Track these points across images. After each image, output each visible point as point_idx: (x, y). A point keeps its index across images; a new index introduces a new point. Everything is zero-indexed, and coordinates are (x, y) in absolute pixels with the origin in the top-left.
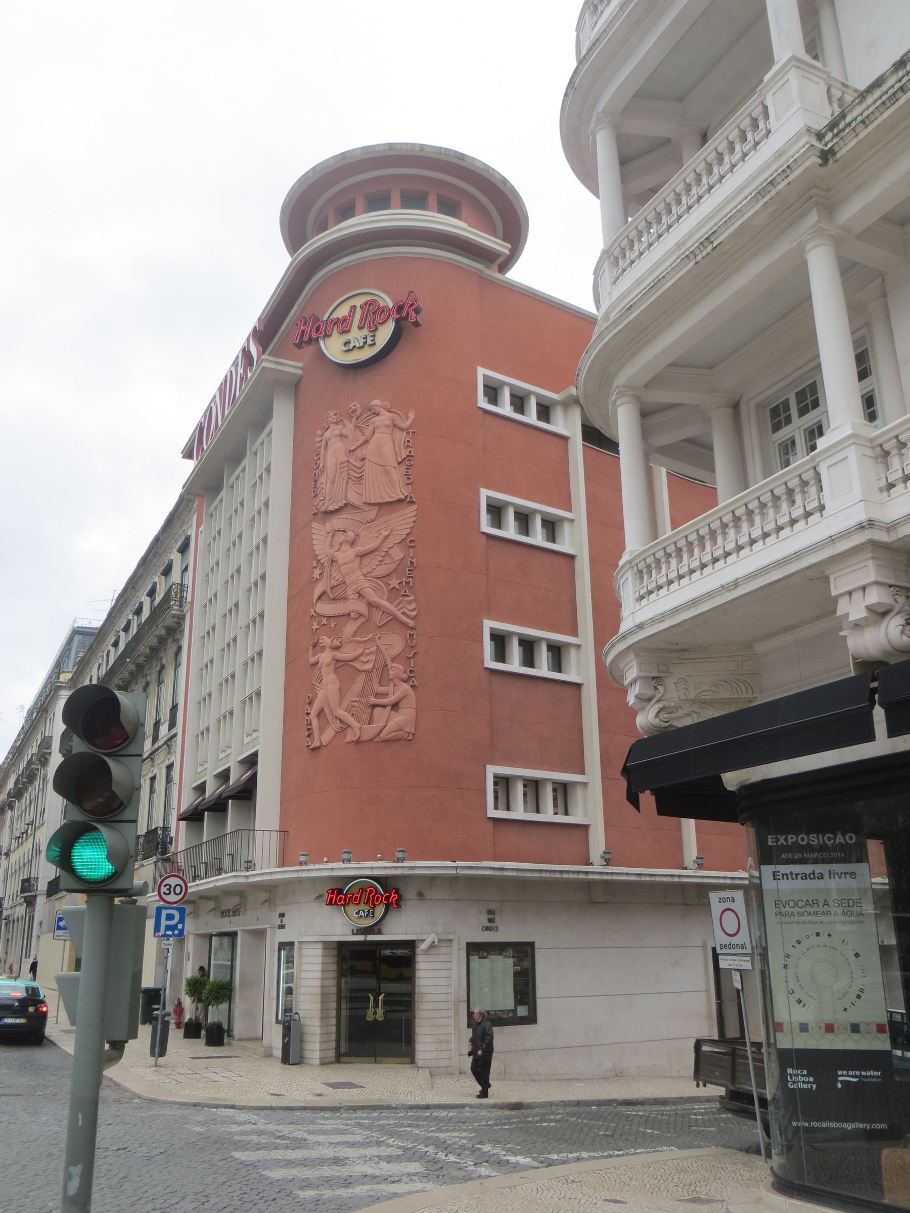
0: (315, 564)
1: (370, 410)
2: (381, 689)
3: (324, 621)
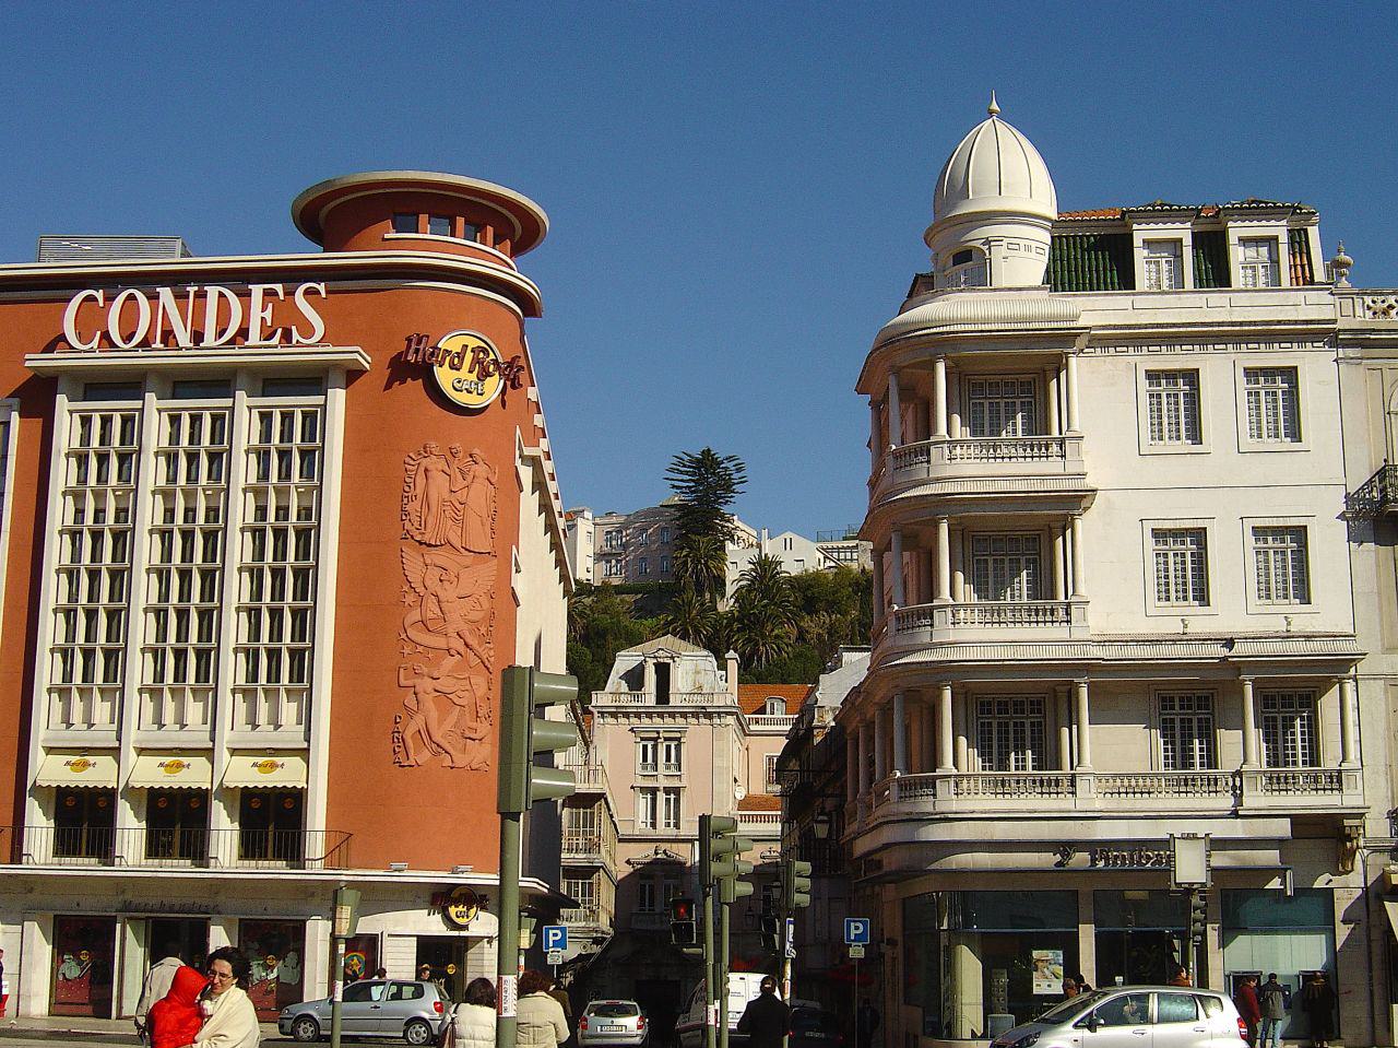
0: (406, 588)
1: (471, 456)
2: (474, 725)
3: (420, 649)
